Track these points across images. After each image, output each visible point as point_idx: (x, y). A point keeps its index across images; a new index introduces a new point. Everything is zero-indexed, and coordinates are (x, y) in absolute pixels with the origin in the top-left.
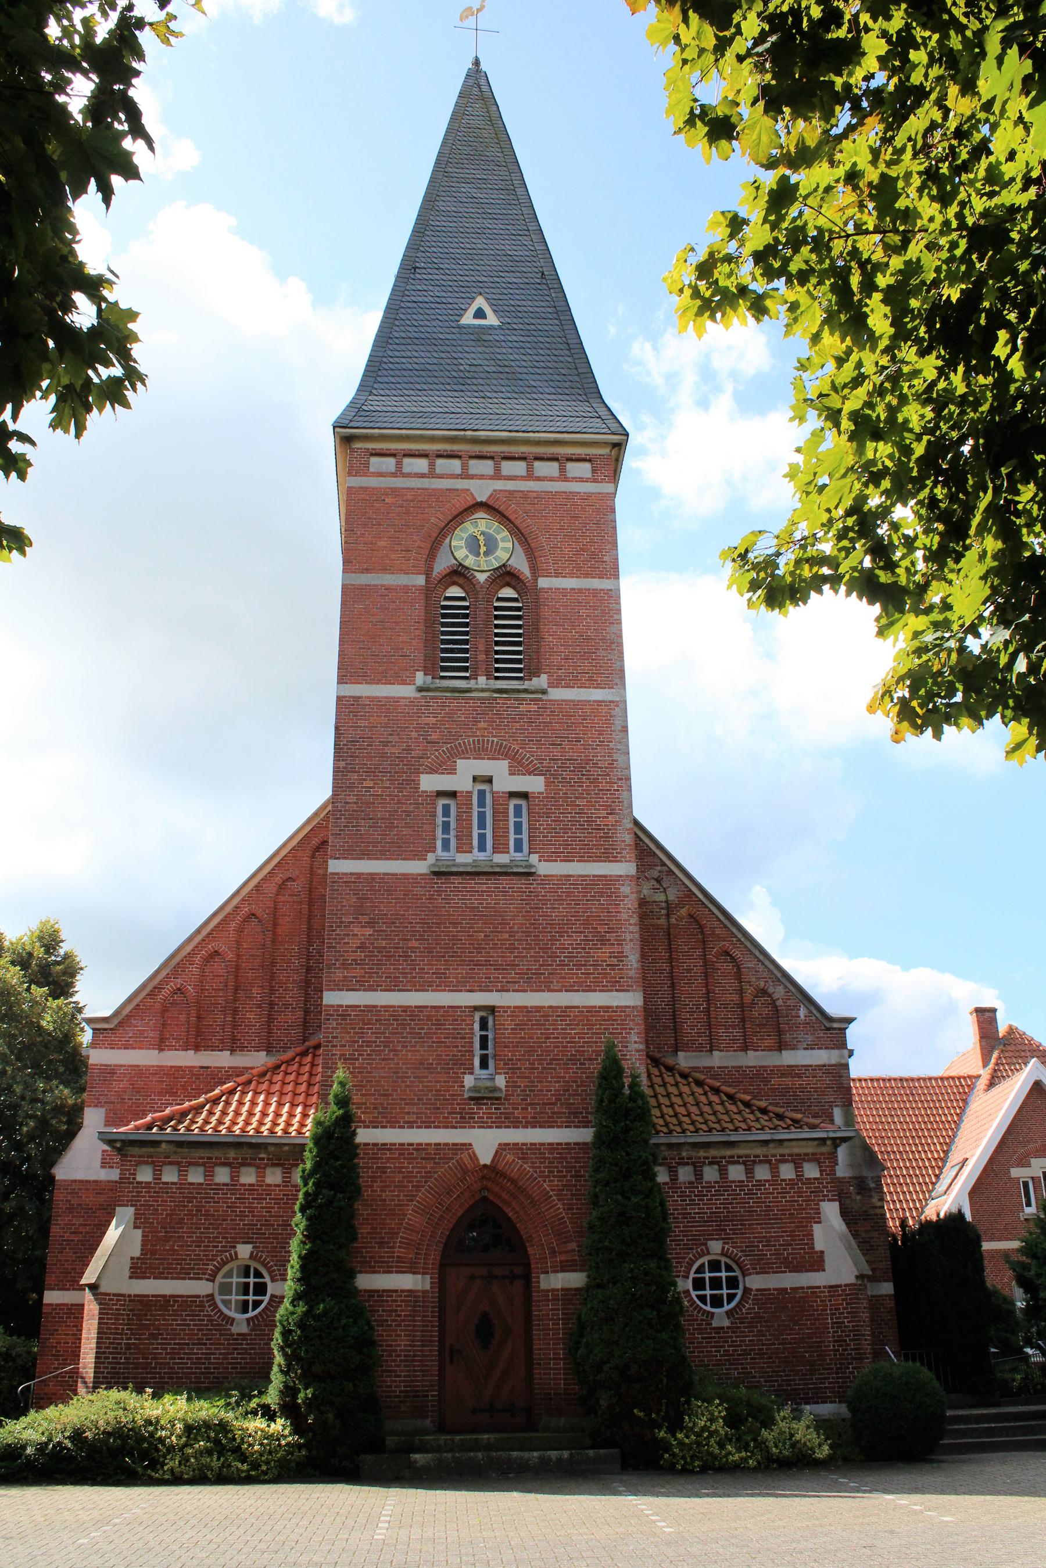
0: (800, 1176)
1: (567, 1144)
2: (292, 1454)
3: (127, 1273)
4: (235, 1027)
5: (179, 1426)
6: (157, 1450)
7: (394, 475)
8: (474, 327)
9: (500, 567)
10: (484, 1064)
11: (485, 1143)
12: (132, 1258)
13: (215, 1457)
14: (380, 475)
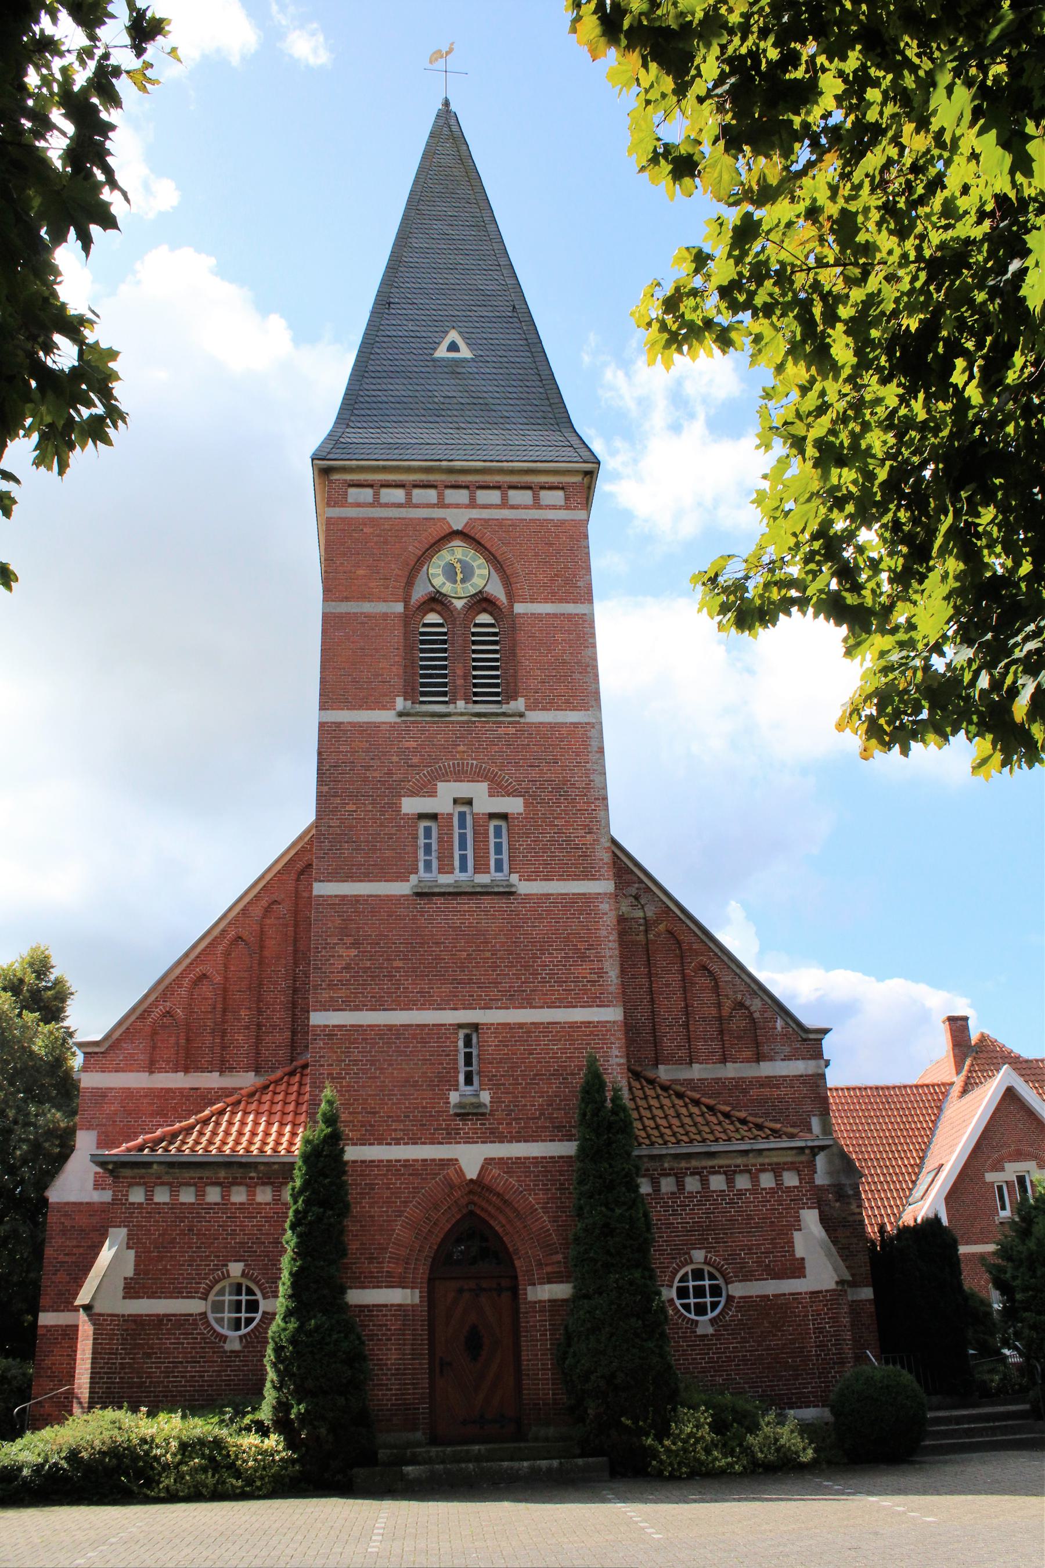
0: (779, 1184)
1: (550, 1158)
2: (286, 1469)
3: (121, 1294)
4: (224, 1048)
5: (174, 1444)
6: (153, 1468)
7: (371, 505)
8: (448, 360)
9: (476, 594)
10: (469, 1081)
11: (471, 1158)
12: (125, 1279)
13: (210, 1474)
14: (358, 505)
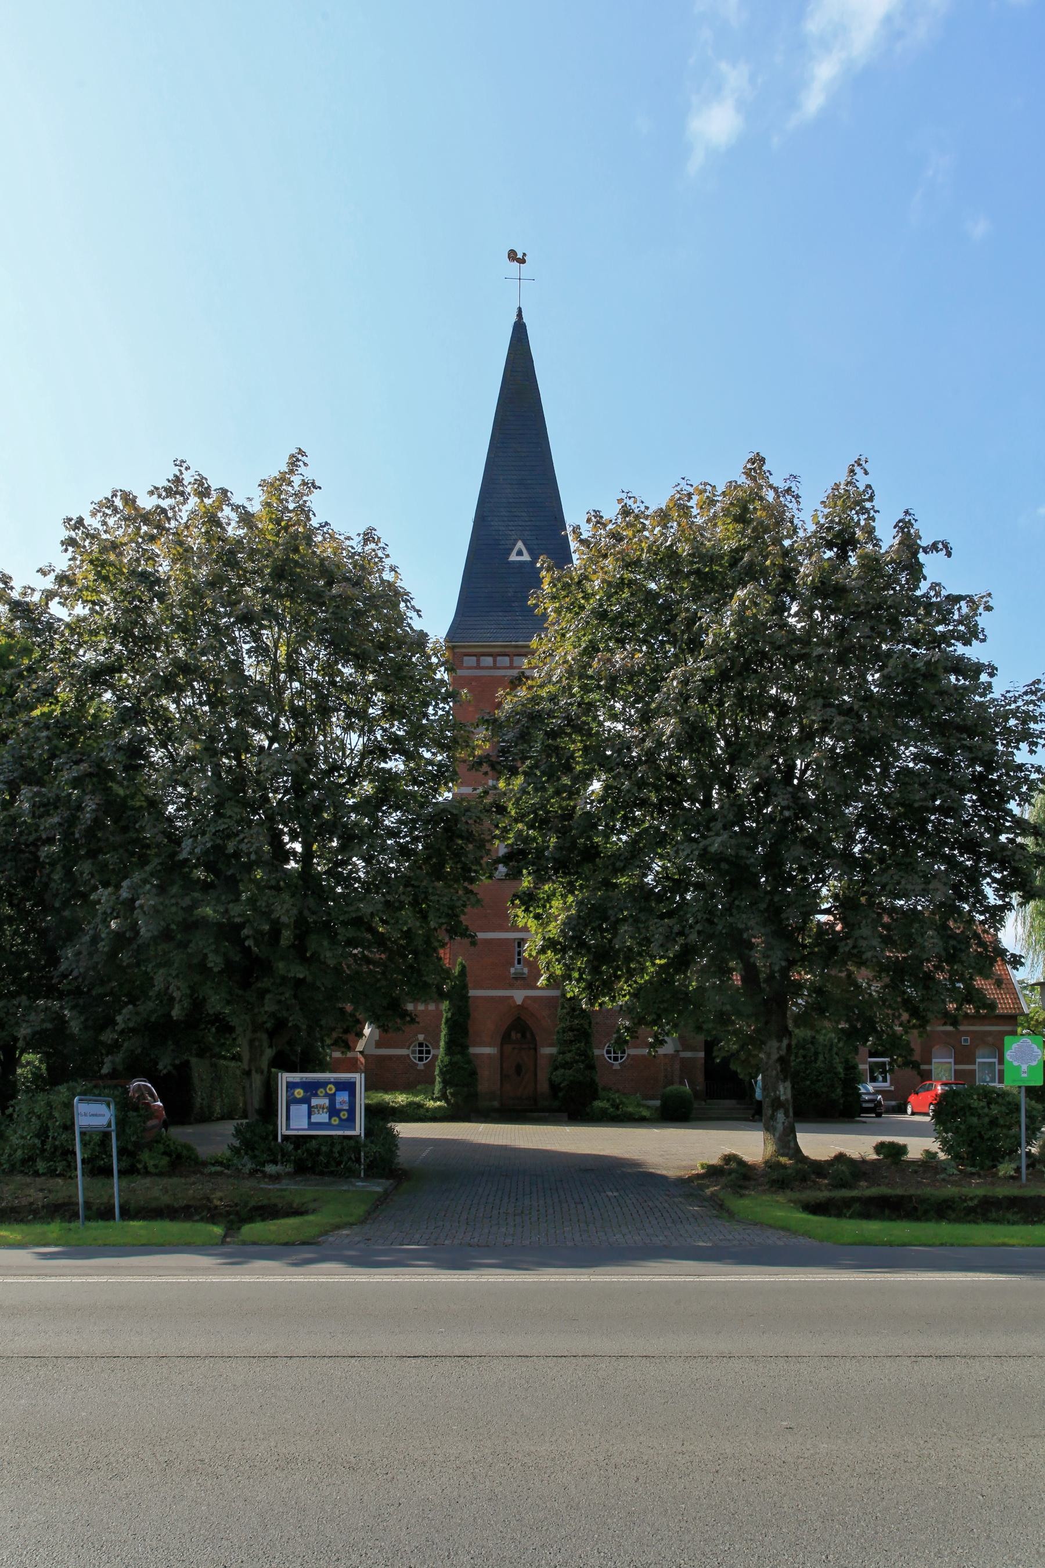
10: (519, 963)
